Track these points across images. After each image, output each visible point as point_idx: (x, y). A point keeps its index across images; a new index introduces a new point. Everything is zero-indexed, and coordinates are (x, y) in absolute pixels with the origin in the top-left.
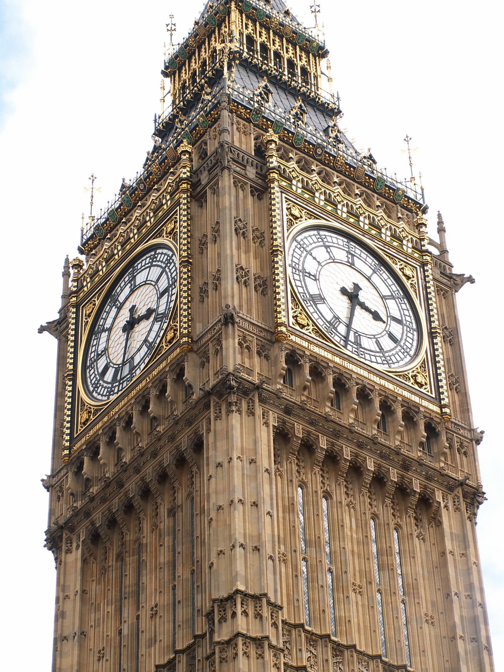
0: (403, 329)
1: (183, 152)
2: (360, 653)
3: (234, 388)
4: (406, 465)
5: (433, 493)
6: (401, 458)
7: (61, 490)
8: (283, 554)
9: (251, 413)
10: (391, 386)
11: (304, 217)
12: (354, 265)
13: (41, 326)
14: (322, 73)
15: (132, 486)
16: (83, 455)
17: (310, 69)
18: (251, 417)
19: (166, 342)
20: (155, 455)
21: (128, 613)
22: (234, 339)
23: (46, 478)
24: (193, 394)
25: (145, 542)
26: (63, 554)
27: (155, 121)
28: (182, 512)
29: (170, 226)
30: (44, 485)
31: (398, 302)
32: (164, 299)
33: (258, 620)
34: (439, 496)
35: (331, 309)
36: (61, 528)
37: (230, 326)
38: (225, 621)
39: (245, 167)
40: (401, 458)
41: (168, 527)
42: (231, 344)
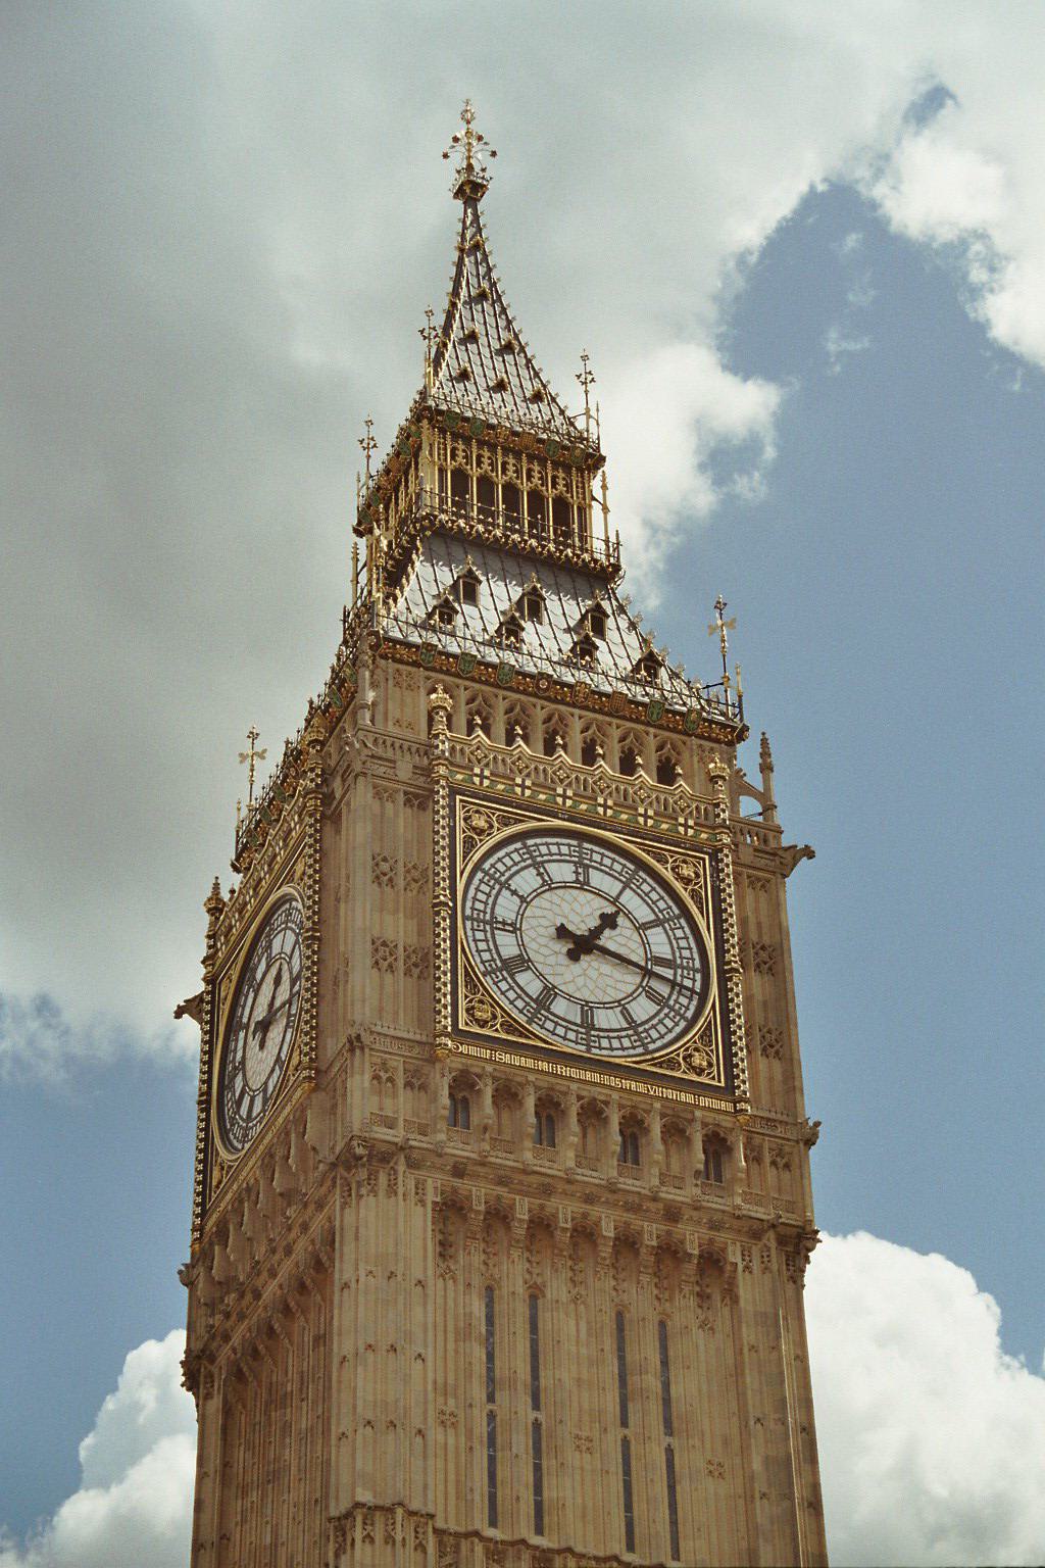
1: (311, 742)
2: (582, 1556)
4: (672, 1214)
5: (724, 1250)
6: (661, 1206)
8: (452, 1414)
9: (392, 1190)
10: (642, 1088)
11: (496, 825)
12: (588, 884)
13: (179, 1006)
14: (594, 499)
17: (572, 497)
18: (393, 1198)
22: (363, 1073)
27: (345, 621)
28: (325, 1345)
29: (299, 868)
31: (668, 928)
33: (389, 1547)
34: (734, 1255)
35: (540, 976)
37: (358, 1052)
39: (394, 762)
42: (359, 1083)
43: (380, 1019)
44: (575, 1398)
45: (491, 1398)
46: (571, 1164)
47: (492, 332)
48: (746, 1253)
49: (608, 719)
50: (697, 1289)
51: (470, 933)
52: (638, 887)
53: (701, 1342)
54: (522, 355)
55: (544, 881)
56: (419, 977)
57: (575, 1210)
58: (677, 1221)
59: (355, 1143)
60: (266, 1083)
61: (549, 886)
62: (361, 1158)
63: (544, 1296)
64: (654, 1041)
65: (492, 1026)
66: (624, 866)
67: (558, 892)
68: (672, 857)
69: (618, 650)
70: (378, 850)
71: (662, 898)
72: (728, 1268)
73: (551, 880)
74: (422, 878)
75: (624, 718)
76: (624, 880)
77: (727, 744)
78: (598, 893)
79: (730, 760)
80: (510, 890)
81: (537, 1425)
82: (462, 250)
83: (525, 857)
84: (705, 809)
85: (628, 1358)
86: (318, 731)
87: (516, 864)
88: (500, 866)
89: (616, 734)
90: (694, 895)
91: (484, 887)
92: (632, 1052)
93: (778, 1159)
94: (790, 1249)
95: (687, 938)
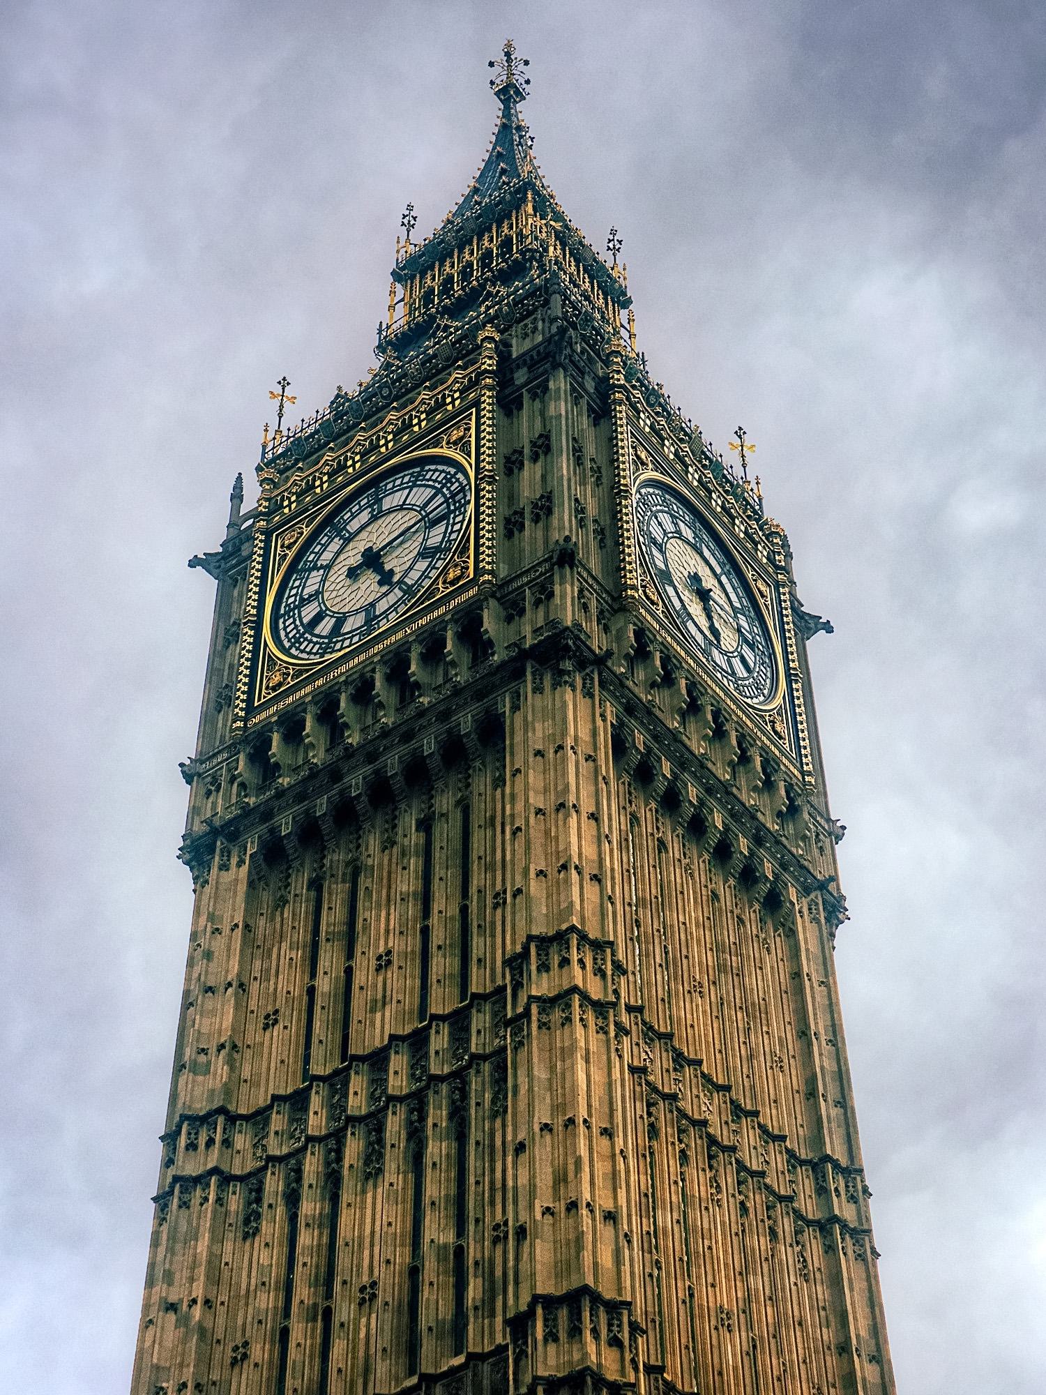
7: (215, 781)
14: (622, 326)
15: (356, 782)
16: (271, 731)
18: (588, 700)
19: (444, 583)
20: (407, 737)
21: (330, 959)
23: (188, 762)
24: (493, 654)
25: (370, 861)
26: (214, 870)
27: (380, 331)
30: (183, 772)
32: (440, 529)
33: (598, 977)
34: (793, 894)
36: (214, 832)
38: (548, 970)
40: (756, 823)
41: (416, 845)
60: (372, 605)
61: (679, 535)
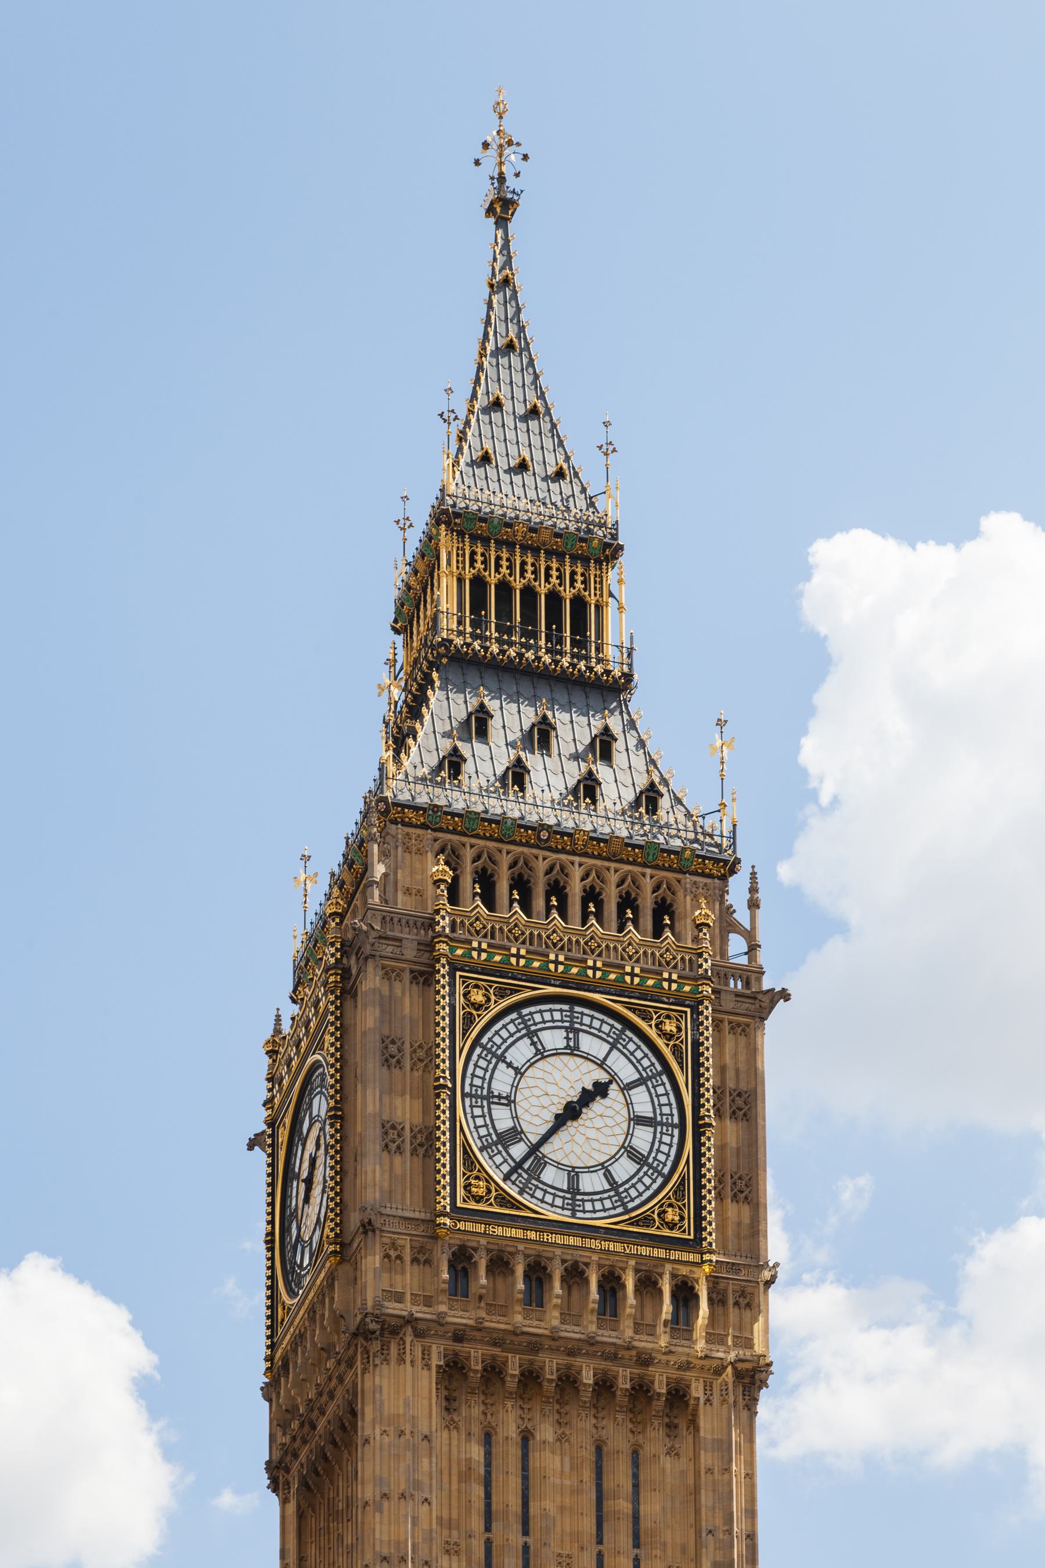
0: (655, 1133)
1: (331, 915)
3: (375, 1332)
6: (634, 1353)
9: (401, 1360)
10: (619, 1247)
34: (697, 1391)
37: (370, 1233)
40: (634, 1353)
42: (372, 1261)
43: (391, 1202)
44: (558, 1524)
45: (488, 1529)
46: (556, 1322)
47: (518, 393)
48: (708, 1387)
49: (606, 864)
50: (667, 1420)
51: (468, 1110)
52: (625, 1047)
53: (668, 1466)
54: (547, 418)
55: (537, 1050)
56: (424, 1156)
57: (560, 1361)
58: (648, 1366)
59: (368, 1320)
61: (541, 1054)
62: (375, 1332)
63: (534, 1437)
64: (632, 1200)
65: (487, 1200)
66: (612, 1026)
67: (550, 1059)
68: (656, 1013)
69: (624, 777)
70: (387, 1033)
71: (646, 1056)
72: (692, 1402)
73: (544, 1048)
74: (427, 1058)
75: (621, 861)
76: (611, 1040)
77: (719, 878)
78: (587, 1058)
79: (724, 892)
80: (506, 1063)
81: (526, 1548)
82: (491, 286)
83: (520, 1027)
84: (690, 960)
85: (605, 1486)
86: (337, 903)
87: (511, 1035)
88: (497, 1040)
89: (613, 878)
90: (677, 1051)
91: (482, 1063)
92: (612, 1212)
93: (741, 1300)
94: (747, 1380)
95: (667, 1094)
